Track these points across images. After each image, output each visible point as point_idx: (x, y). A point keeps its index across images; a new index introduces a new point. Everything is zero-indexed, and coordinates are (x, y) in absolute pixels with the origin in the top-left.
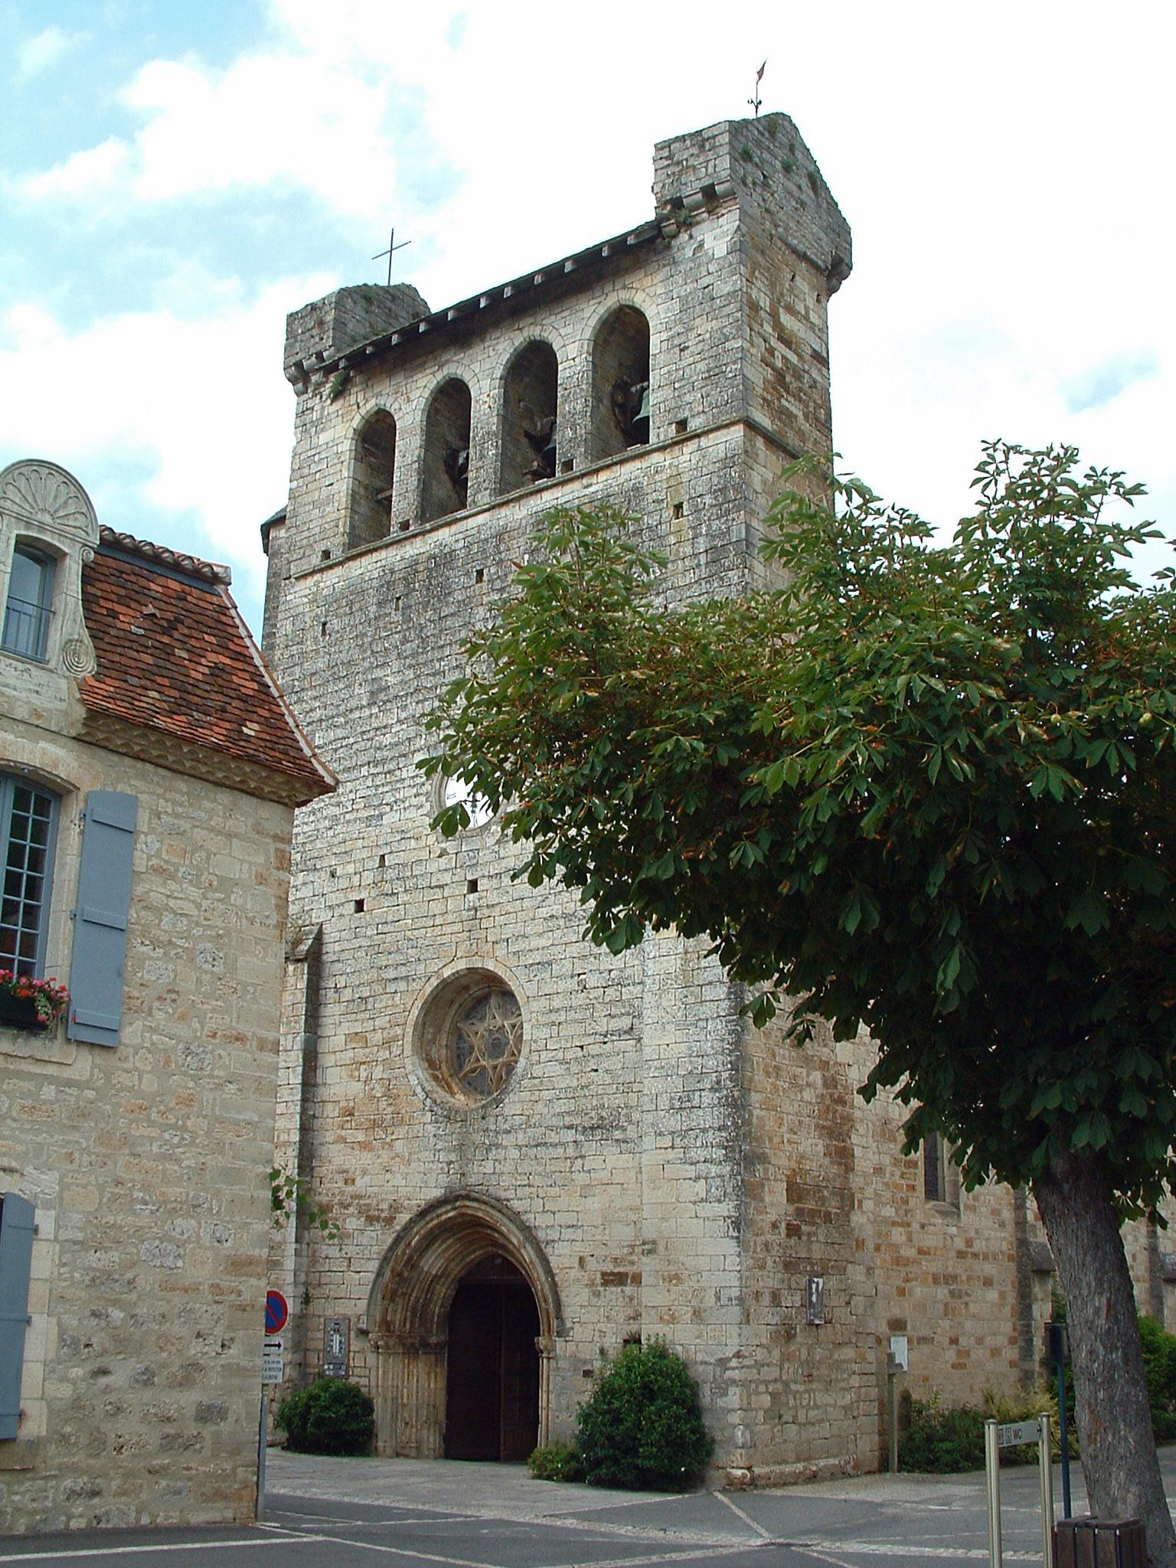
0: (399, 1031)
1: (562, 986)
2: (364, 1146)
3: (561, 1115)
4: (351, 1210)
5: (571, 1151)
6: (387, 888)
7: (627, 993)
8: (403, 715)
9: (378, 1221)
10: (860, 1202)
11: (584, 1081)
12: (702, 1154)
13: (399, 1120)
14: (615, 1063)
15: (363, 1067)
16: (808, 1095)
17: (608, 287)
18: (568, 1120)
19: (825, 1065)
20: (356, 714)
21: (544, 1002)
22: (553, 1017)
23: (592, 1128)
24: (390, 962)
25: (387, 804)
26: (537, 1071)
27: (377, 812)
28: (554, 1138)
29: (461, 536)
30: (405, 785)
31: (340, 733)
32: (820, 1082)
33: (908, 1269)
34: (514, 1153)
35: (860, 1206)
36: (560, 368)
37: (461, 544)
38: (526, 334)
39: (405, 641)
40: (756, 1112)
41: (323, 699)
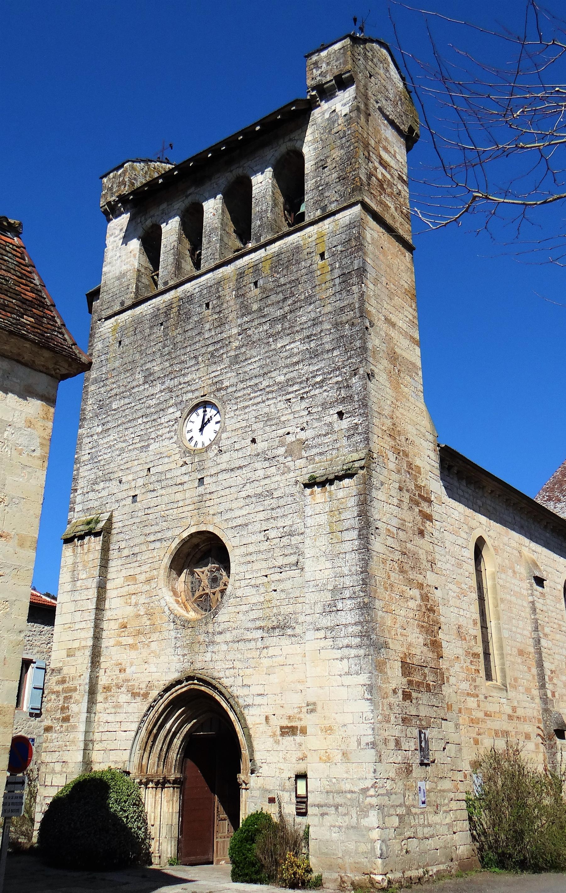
0: (155, 572)
1: (253, 538)
2: (132, 647)
3: (254, 620)
4: (123, 689)
5: (260, 644)
6: (151, 487)
7: (295, 540)
8: (163, 387)
9: (139, 696)
10: (448, 678)
11: (267, 598)
12: (346, 641)
13: (154, 628)
14: (288, 585)
15: (133, 596)
16: (412, 604)
17: (281, 141)
18: (259, 623)
19: (421, 586)
20: (136, 390)
21: (243, 550)
22: (249, 558)
23: (273, 628)
24: (151, 531)
25: (152, 439)
26: (239, 593)
27: (146, 444)
28: (249, 635)
29: (197, 286)
30: (163, 426)
31: (127, 401)
32: (418, 597)
33: (480, 726)
34: (224, 647)
35: (448, 681)
36: (253, 188)
37: (197, 290)
38: (234, 172)
39: (164, 346)
40: (380, 613)
41: (118, 383)
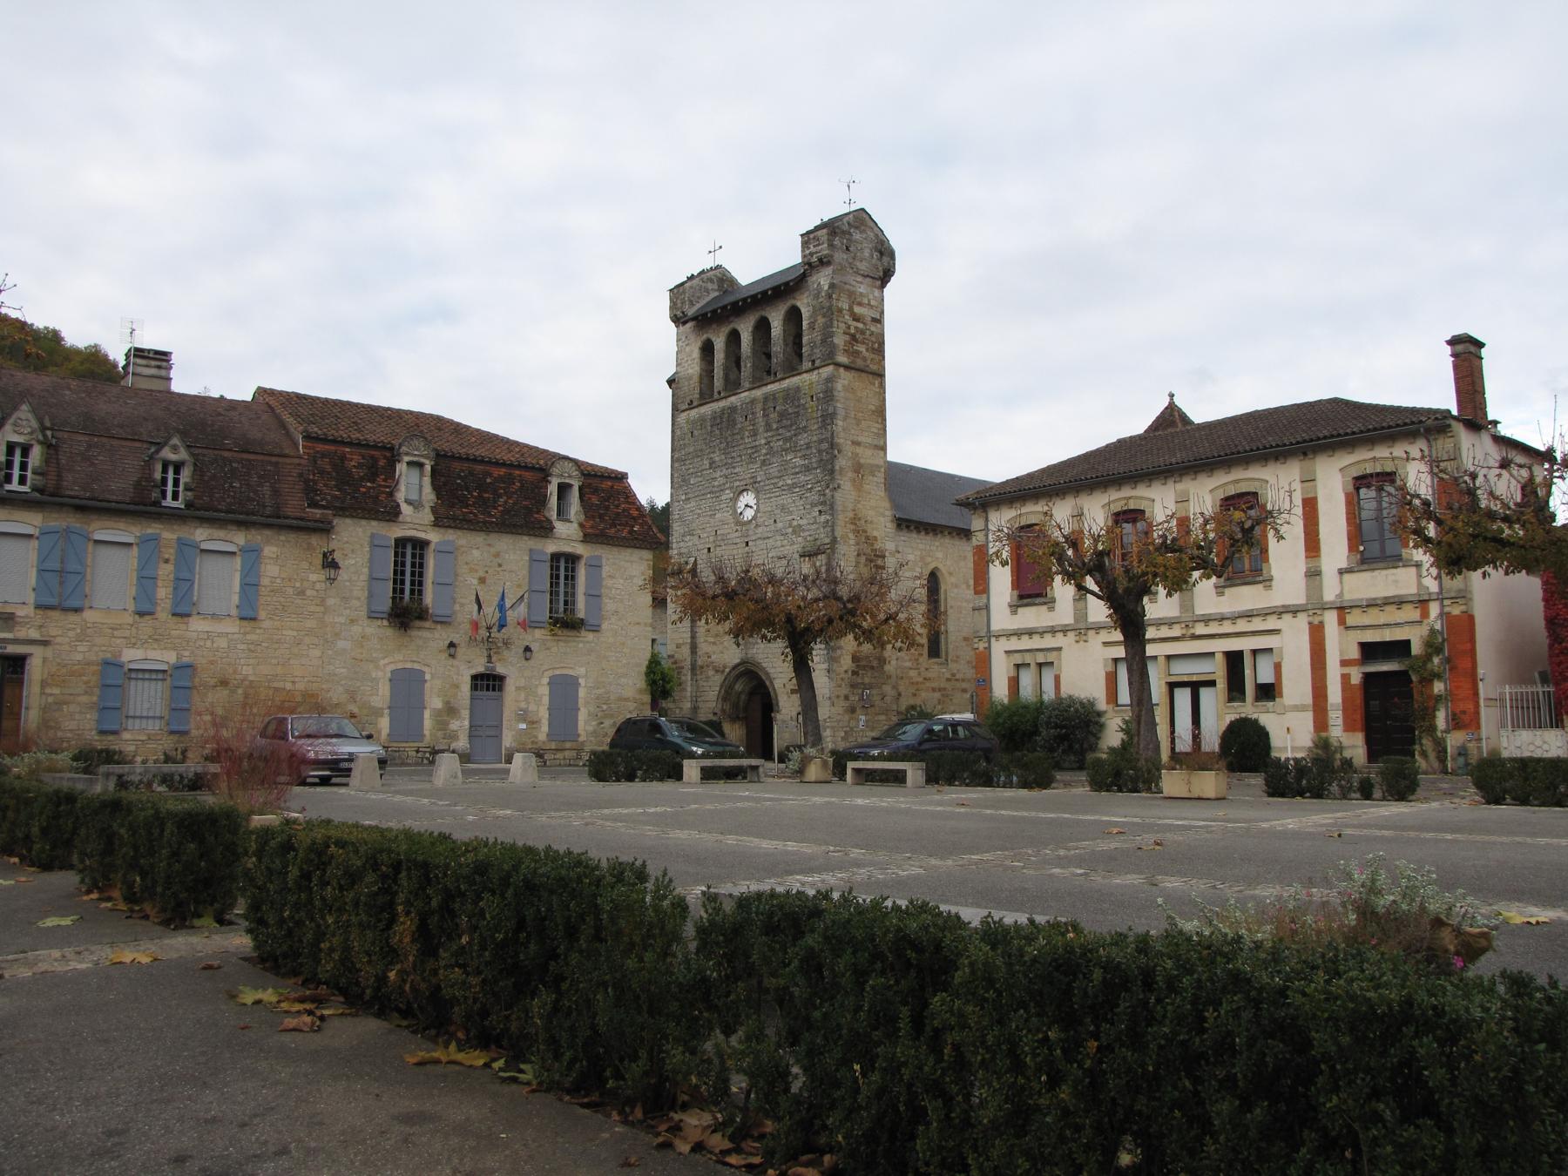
2: (714, 643)
31: (700, 479)
